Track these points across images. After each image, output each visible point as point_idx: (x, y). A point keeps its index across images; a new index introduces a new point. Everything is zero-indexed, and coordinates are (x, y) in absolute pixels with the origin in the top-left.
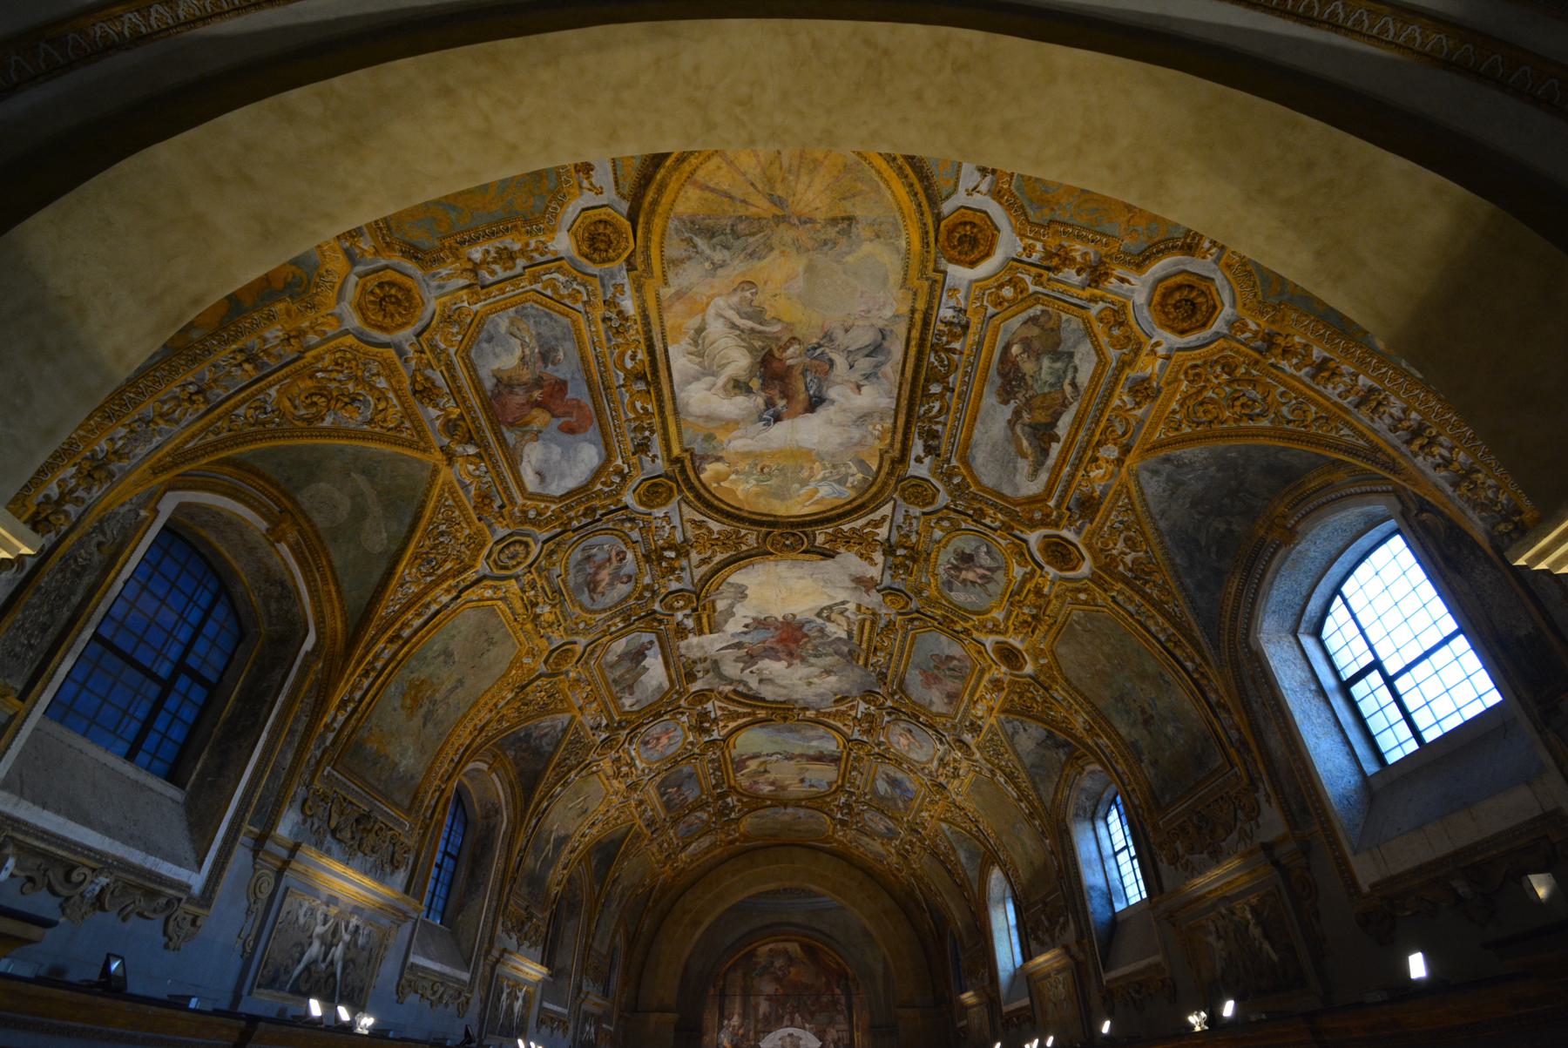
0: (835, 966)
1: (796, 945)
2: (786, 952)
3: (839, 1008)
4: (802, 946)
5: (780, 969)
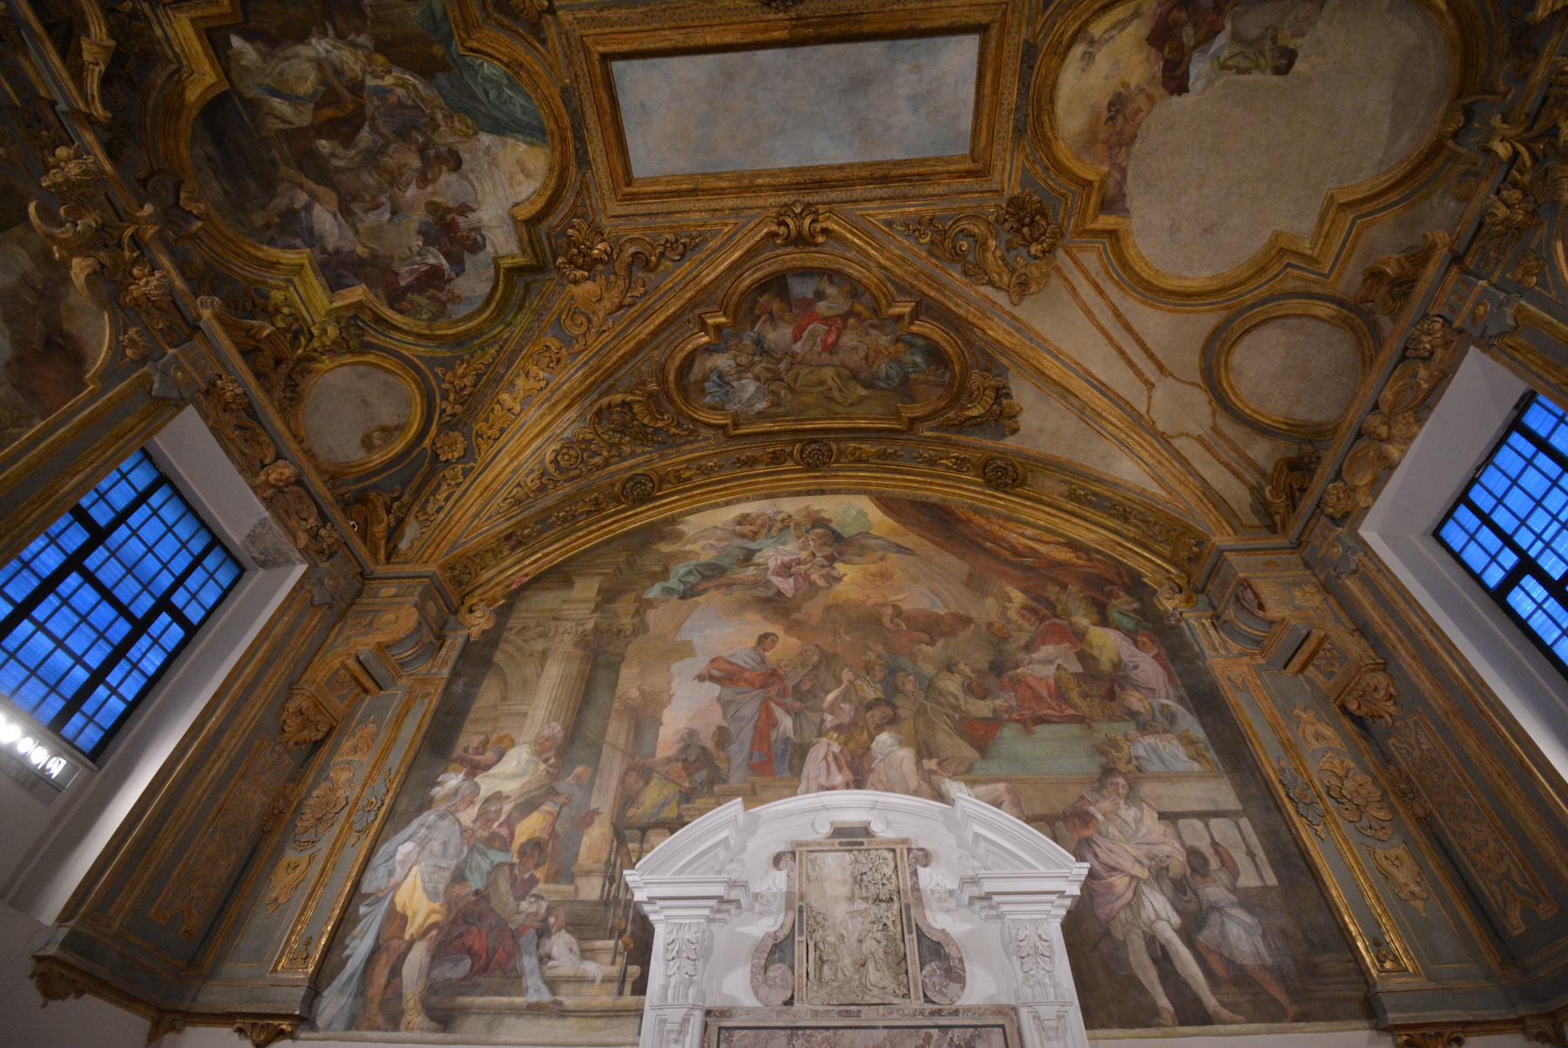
1: (865, 504)
2: (819, 522)
3: (1134, 700)
4: (888, 504)
5: (785, 570)
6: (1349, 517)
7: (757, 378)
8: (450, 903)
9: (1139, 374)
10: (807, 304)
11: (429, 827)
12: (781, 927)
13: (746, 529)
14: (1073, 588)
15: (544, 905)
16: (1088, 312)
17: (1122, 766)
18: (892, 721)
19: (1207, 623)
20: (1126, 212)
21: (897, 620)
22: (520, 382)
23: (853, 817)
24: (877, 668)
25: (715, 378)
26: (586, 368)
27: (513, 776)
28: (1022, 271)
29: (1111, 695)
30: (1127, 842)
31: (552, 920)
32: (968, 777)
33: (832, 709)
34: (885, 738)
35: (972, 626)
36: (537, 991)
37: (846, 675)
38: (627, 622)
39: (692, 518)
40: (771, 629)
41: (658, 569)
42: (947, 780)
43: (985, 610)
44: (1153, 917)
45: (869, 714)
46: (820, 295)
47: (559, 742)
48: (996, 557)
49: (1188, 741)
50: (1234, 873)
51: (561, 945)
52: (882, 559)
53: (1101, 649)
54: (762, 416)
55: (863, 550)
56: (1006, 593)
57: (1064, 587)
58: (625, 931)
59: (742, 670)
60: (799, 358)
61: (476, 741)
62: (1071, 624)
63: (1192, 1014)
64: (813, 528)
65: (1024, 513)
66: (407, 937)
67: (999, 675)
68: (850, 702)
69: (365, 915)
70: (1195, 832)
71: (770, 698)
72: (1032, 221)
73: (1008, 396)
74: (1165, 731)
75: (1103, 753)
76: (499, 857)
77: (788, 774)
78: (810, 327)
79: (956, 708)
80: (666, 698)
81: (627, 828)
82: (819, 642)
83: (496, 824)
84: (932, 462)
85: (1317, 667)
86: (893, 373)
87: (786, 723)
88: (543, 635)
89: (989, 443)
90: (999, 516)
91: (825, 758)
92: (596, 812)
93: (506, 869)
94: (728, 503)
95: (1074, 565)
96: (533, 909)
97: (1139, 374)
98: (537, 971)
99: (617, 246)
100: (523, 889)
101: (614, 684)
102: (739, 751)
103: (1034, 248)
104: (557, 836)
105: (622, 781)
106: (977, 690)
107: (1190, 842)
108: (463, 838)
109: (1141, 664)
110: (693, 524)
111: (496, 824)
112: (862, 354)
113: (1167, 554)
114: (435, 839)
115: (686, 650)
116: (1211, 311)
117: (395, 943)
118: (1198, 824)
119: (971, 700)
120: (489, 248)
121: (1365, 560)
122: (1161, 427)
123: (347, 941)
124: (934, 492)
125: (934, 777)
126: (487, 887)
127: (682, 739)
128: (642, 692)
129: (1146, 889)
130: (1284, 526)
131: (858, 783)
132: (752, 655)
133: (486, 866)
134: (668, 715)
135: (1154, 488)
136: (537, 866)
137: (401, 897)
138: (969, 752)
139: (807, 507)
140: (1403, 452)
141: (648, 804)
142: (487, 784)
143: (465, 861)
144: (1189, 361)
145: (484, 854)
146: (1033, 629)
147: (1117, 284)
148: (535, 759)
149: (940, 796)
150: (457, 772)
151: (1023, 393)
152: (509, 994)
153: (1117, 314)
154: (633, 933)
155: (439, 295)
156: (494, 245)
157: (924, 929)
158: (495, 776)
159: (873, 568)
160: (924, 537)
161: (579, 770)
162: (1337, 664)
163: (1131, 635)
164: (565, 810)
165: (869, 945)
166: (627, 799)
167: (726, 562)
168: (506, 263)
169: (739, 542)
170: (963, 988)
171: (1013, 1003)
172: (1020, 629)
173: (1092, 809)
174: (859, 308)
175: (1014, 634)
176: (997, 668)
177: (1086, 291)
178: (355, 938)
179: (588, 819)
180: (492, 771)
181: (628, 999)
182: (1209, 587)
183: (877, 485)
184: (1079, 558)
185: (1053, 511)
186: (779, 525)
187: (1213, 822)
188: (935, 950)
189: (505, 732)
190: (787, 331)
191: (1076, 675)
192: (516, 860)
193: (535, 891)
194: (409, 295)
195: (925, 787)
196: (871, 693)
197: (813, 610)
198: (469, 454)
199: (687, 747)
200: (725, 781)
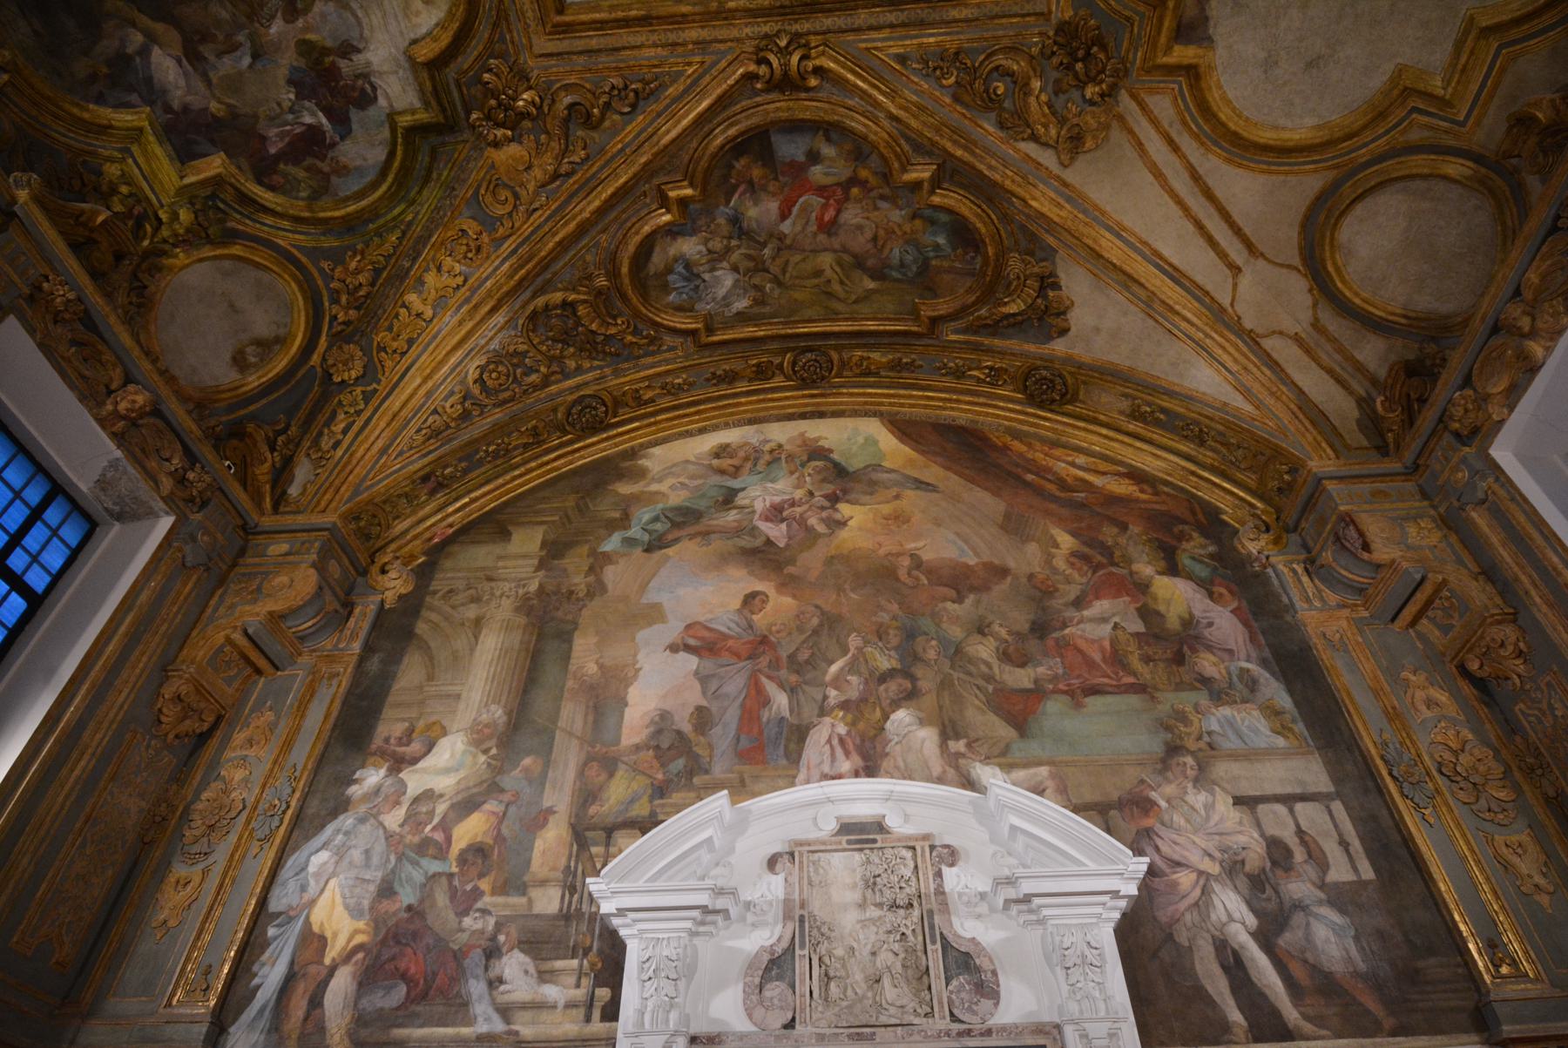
0: (1123, 488)
1: (874, 429)
2: (817, 453)
3: (1208, 664)
4: (904, 429)
5: (776, 513)
6: (1480, 433)
7: (735, 269)
8: (377, 922)
9: (1222, 255)
10: (798, 170)
11: (347, 833)
12: (779, 940)
13: (726, 463)
14: (1135, 529)
15: (492, 921)
16: (1158, 175)
17: (1191, 744)
18: (910, 696)
19: (1299, 569)
20: (1206, 41)
21: (915, 573)
22: (431, 278)
23: (863, 811)
24: (892, 632)
25: (680, 268)
26: (513, 260)
27: (447, 771)
28: (1075, 121)
29: (1179, 659)
30: (1196, 832)
31: (502, 938)
32: (1003, 760)
33: (837, 682)
34: (902, 717)
35: (1009, 579)
36: (489, 1020)
37: (854, 641)
38: (579, 581)
39: (656, 451)
40: (759, 586)
41: (617, 515)
42: (978, 764)
43: (1026, 559)
44: (1224, 918)
45: (882, 688)
46: (814, 157)
47: (501, 728)
48: (1039, 491)
49: (1272, 712)
50: (1323, 865)
51: (514, 966)
52: (897, 497)
53: (1168, 602)
54: (742, 318)
55: (873, 487)
56: (1052, 537)
57: (1124, 527)
58: (590, 948)
59: (725, 637)
60: (788, 242)
61: (398, 729)
62: (1131, 573)
64: (809, 460)
65: (1075, 437)
66: (327, 961)
67: (1041, 638)
68: (860, 674)
69: (275, 938)
70: (1279, 822)
71: (759, 671)
72: (1088, 54)
73: (1056, 286)
74: (1244, 701)
75: (1168, 728)
76: (435, 867)
77: (784, 762)
78: (801, 200)
79: (989, 678)
80: (630, 675)
81: (588, 829)
82: (819, 602)
83: (429, 828)
84: (959, 374)
85: (1431, 620)
86: (909, 258)
87: (781, 700)
88: (476, 600)
89: (1031, 348)
90: (1043, 440)
91: (829, 741)
92: (550, 811)
93: (444, 880)
94: (702, 431)
95: (1137, 500)
96: (479, 925)
97: (1222, 255)
98: (487, 997)
99: (548, 94)
100: (465, 903)
101: (566, 658)
102: (723, 735)
103: (1090, 91)
104: (504, 839)
105: (581, 773)
106: (1013, 656)
107: (1271, 831)
108: (389, 845)
109: (1217, 621)
110: (658, 458)
111: (429, 828)
112: (869, 234)
113: (1253, 484)
114: (355, 846)
116: (1315, 171)
117: (313, 969)
118: (1281, 809)
119: (1007, 668)
120: (382, 102)
121: (1496, 487)
122: (1248, 324)
123: (255, 968)
124: (962, 412)
125: (962, 761)
126: (422, 901)
127: (652, 722)
128: (601, 667)
129: (1217, 887)
130: (1398, 447)
131: (870, 769)
132: (736, 619)
133: (418, 876)
134: (633, 694)
135: (1238, 402)
136: (481, 876)
137: (318, 916)
138: (1005, 731)
139: (802, 434)
140: (1549, 350)
141: (613, 801)
142: (415, 781)
143: (393, 871)
144: (1285, 238)
145: (416, 864)
146: (1084, 580)
147: (1196, 137)
148: (473, 749)
149: (969, 783)
150: (377, 767)
151: (1075, 282)
152: (453, 1025)
153: (1196, 177)
154: (600, 952)
155: (319, 164)
156: (387, 97)
157: (950, 938)
158: (424, 770)
159: (886, 509)
160: (948, 469)
161: (527, 761)
162: (1456, 615)
163: (1206, 586)
164: (512, 809)
165: (885, 958)
166: (587, 796)
167: (702, 505)
168: (405, 121)
169: (717, 479)
170: (997, 1004)
171: (1058, 1021)
172: (1068, 581)
173: (1153, 795)
174: (864, 174)
175: (1061, 587)
176: (1040, 629)
177: (1156, 148)
178: (263, 965)
179: (541, 819)
180: (420, 765)
181: (597, 1027)
182: (1303, 524)
183: (891, 404)
184: (1142, 491)
185: (1111, 434)
186: (767, 457)
187: (1299, 807)
188: (962, 961)
189: (434, 718)
190: (773, 206)
191: (1137, 635)
192: (455, 869)
193: (479, 905)
194: (282, 166)
195: (951, 772)
196: (884, 662)
197: (811, 562)
198: (370, 373)
199: (659, 732)
200: (707, 772)
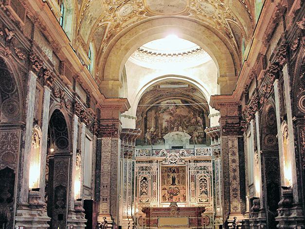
1: (180, 101)
3: (199, 124)
5: (172, 110)
63: (196, 144)
115: (164, 119)
131: (178, 131)
166: (161, 131)
